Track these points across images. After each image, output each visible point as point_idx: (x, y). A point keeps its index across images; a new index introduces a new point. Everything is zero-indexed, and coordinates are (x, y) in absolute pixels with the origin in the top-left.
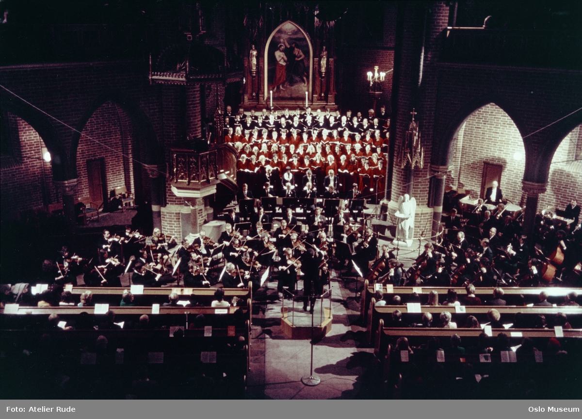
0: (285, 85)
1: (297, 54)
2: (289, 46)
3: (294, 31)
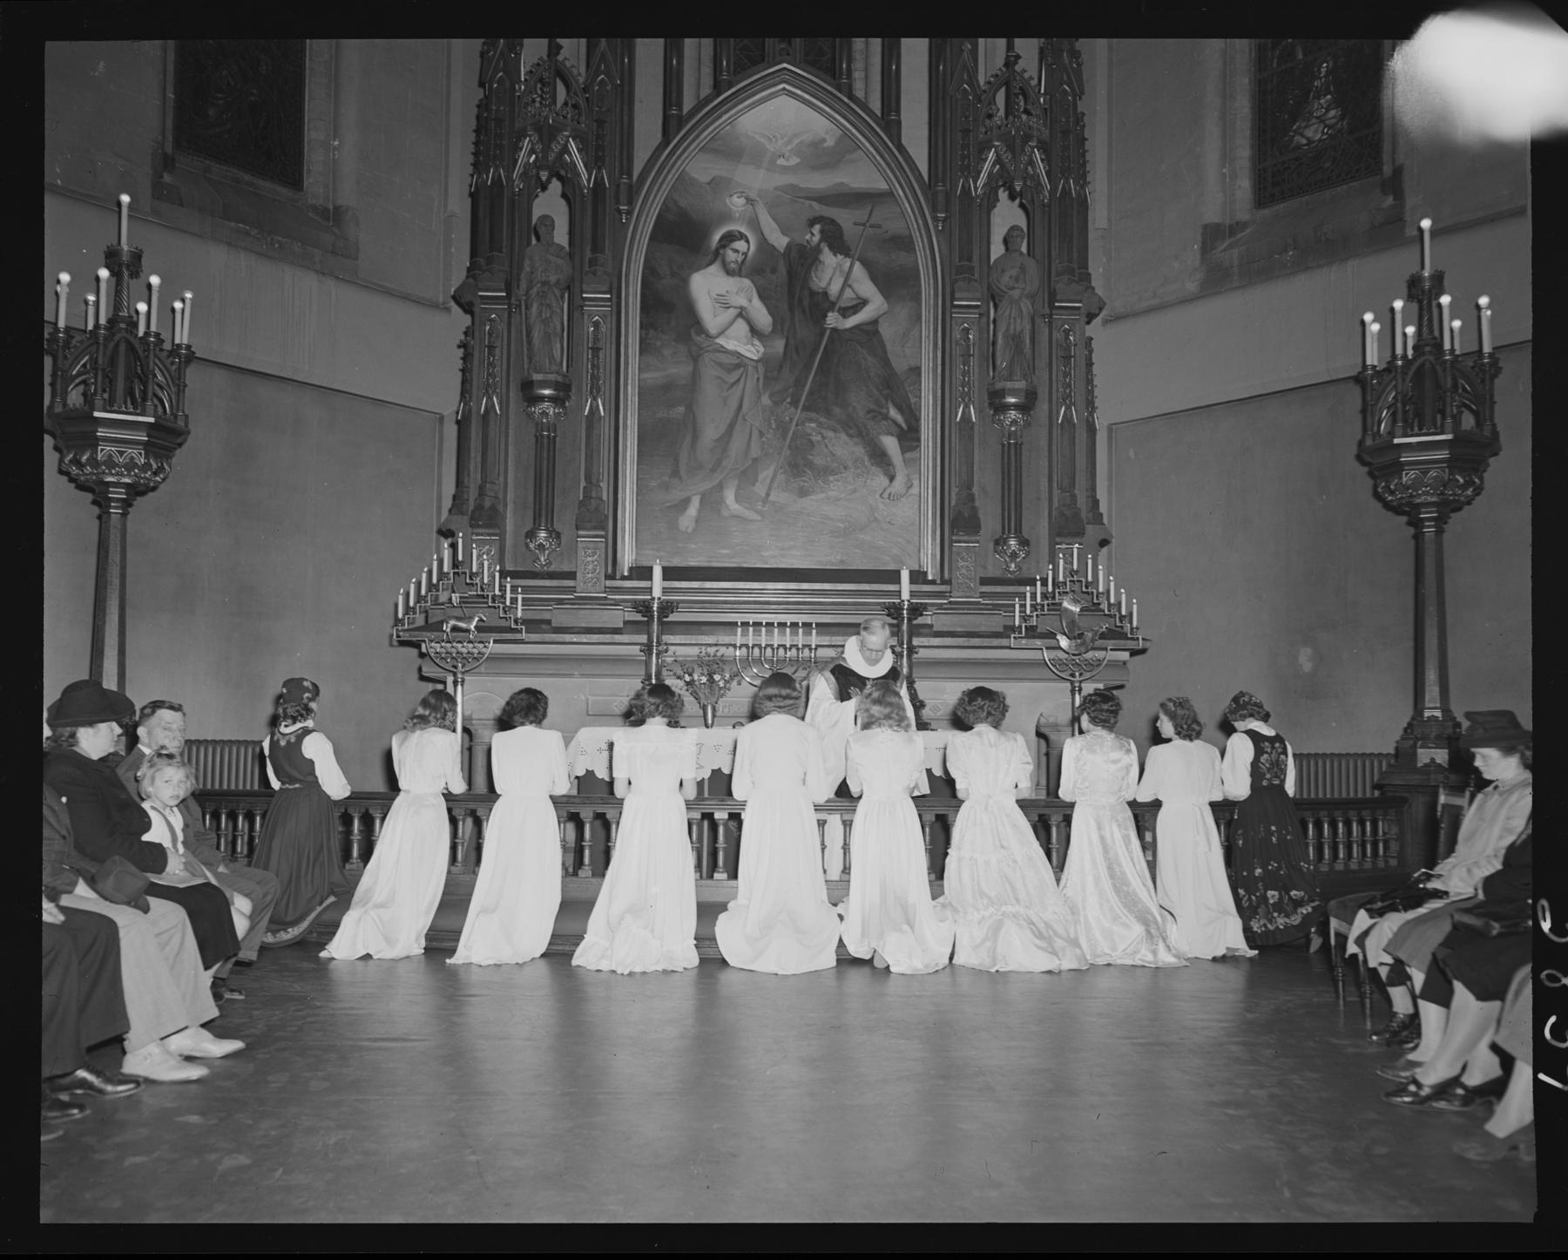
0: (760, 489)
1: (834, 289)
2: (780, 241)
3: (816, 144)
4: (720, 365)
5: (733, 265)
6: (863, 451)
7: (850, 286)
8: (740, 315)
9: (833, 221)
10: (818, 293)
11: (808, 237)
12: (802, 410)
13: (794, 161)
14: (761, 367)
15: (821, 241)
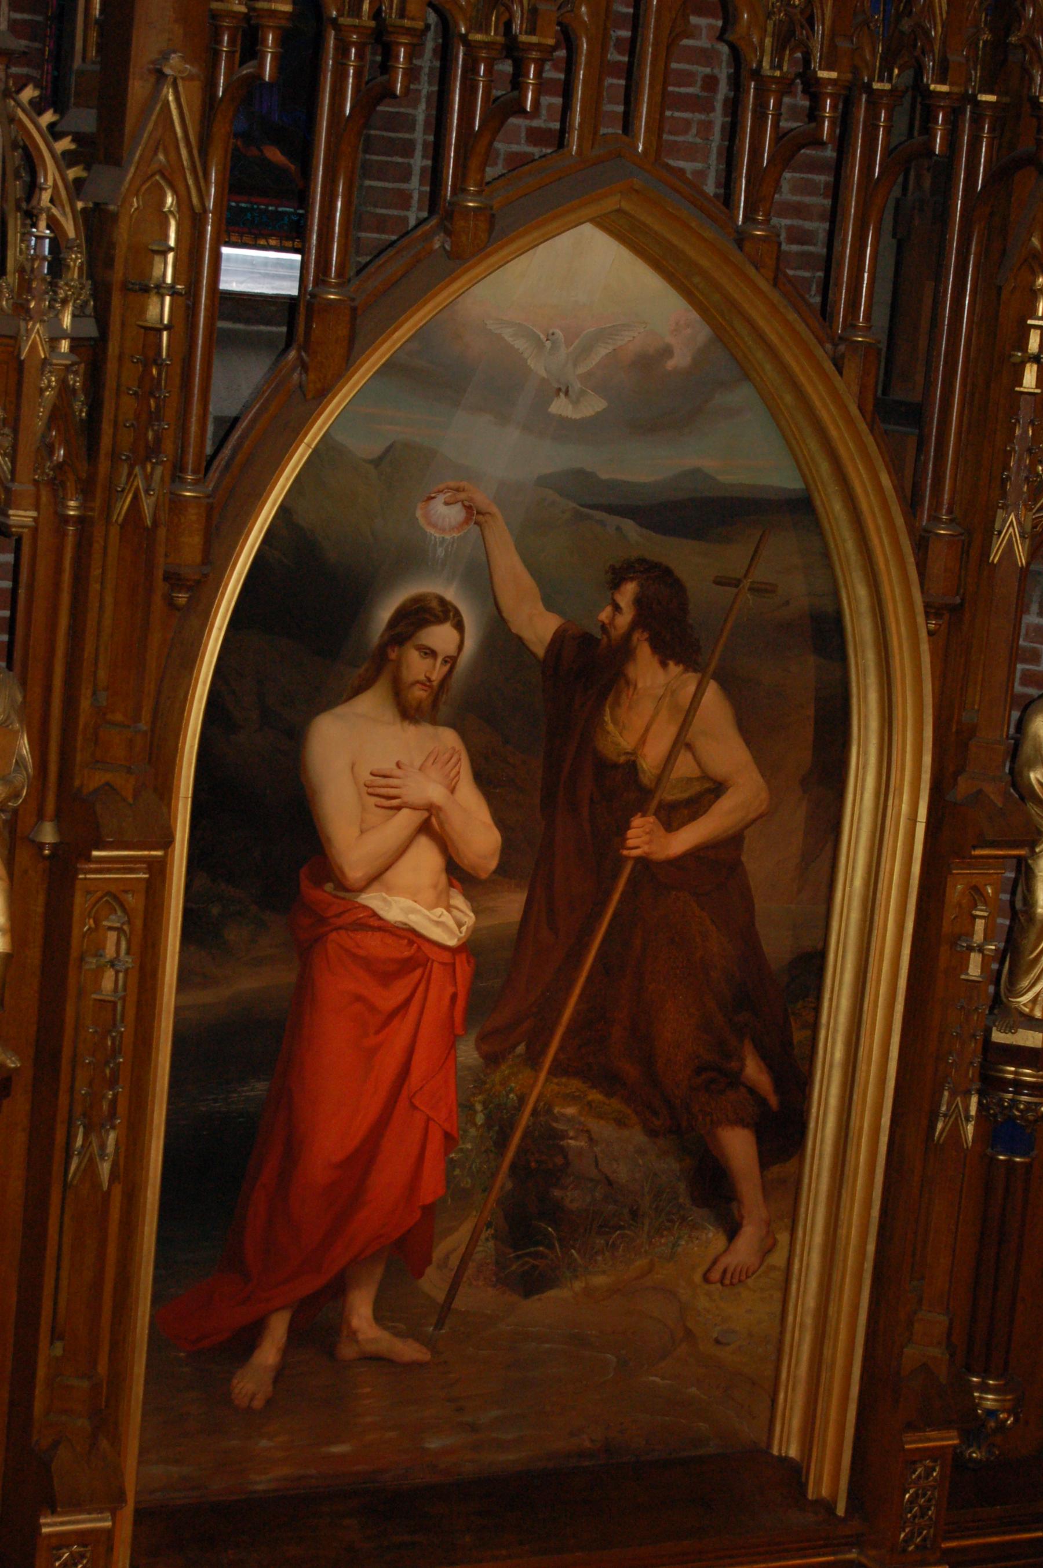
4: (368, 964)
5: (419, 693)
6: (676, 1166)
7: (689, 747)
8: (425, 828)
9: (667, 572)
10: (615, 766)
11: (605, 615)
12: (551, 1073)
13: (593, 406)
14: (464, 970)
15: (634, 625)
